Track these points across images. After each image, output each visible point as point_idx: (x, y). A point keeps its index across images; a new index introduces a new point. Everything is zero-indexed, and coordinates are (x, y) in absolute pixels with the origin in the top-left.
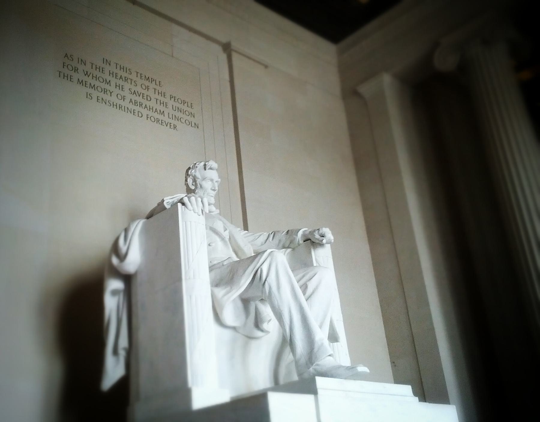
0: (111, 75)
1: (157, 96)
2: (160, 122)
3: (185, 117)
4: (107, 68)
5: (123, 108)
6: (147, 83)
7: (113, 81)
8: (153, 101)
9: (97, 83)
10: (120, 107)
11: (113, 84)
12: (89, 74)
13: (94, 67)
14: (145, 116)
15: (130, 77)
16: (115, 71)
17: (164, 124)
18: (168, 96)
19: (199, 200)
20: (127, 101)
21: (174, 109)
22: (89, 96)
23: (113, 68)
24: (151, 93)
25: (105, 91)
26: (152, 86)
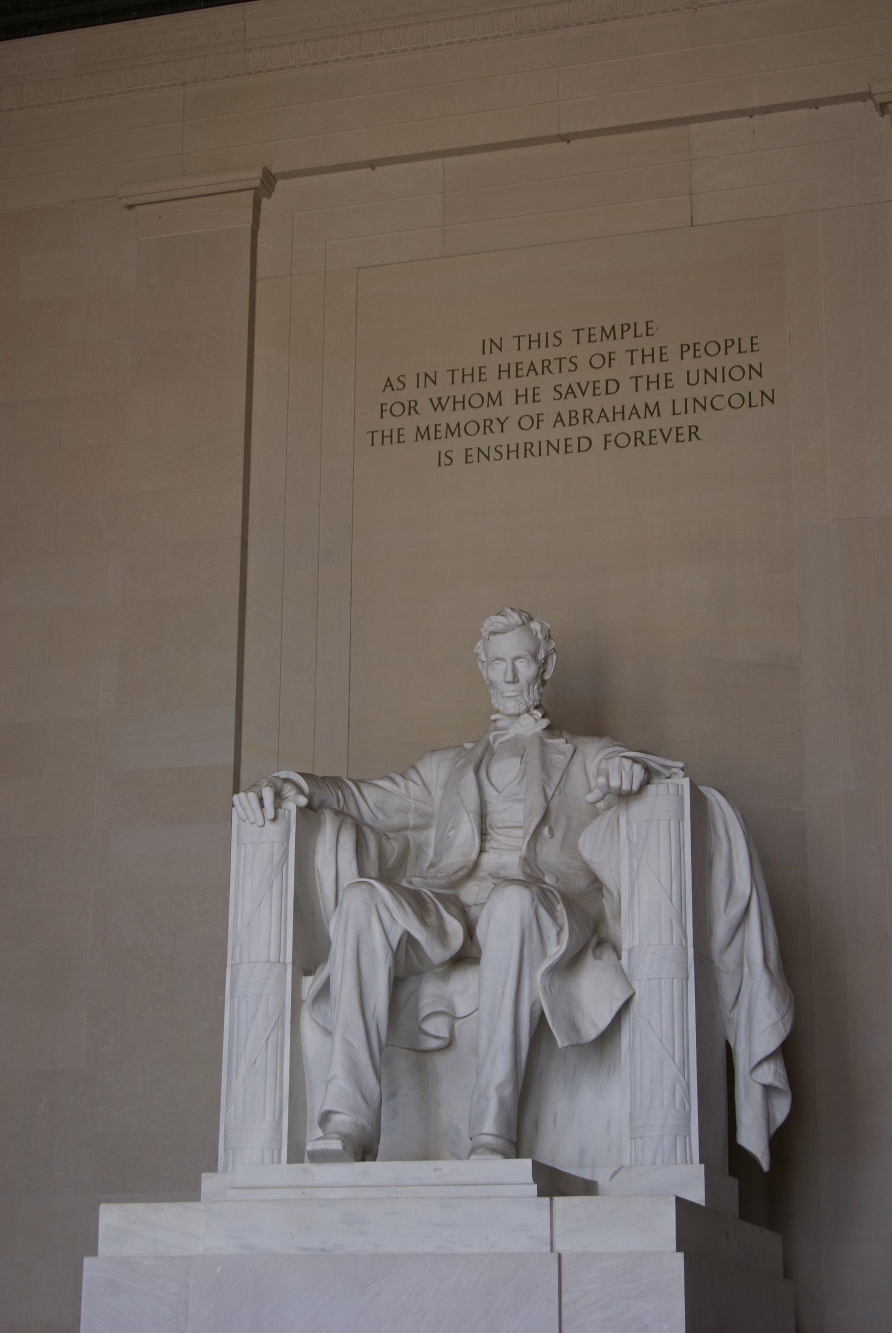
0: (504, 375)
1: (639, 369)
2: (646, 439)
3: (728, 388)
4: (492, 361)
5: (535, 450)
6: (605, 346)
7: (508, 387)
8: (627, 386)
9: (462, 416)
10: (528, 449)
11: (508, 397)
12: (443, 402)
13: (458, 376)
14: (598, 442)
15: (559, 352)
17: (660, 438)
18: (673, 351)
19: (252, 796)
20: (549, 419)
21: (693, 380)
22: (445, 459)
23: (509, 355)
24: (622, 370)
25: (487, 426)
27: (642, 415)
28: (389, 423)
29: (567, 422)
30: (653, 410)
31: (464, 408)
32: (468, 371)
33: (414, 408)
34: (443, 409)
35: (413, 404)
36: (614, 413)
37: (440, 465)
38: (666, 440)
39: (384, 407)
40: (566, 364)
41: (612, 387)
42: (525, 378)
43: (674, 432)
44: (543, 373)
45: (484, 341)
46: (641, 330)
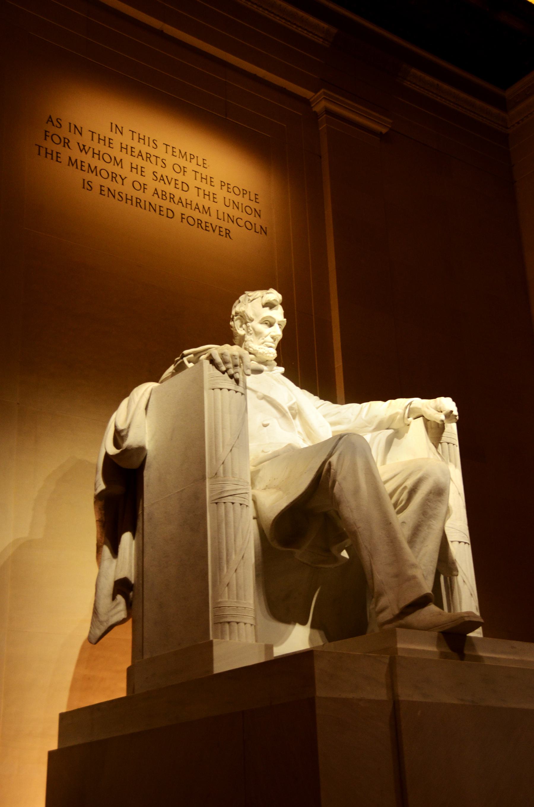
4: (117, 139)
5: (142, 204)
6: (182, 162)
7: (127, 159)
9: (101, 165)
11: (126, 165)
12: (87, 148)
14: (178, 216)
16: (131, 143)
20: (150, 190)
21: (227, 204)
23: (126, 139)
25: (114, 176)
26: (191, 166)
27: (201, 211)
28: (49, 145)
29: (160, 196)
30: (207, 211)
31: (99, 159)
32: (102, 137)
33: (67, 143)
34: (86, 153)
35: (66, 141)
36: (187, 204)
37: (84, 188)
38: (214, 231)
39: (47, 134)
40: (159, 160)
41: (185, 188)
42: (135, 158)
43: (218, 228)
44: (147, 161)
45: (112, 123)
46: (200, 162)
